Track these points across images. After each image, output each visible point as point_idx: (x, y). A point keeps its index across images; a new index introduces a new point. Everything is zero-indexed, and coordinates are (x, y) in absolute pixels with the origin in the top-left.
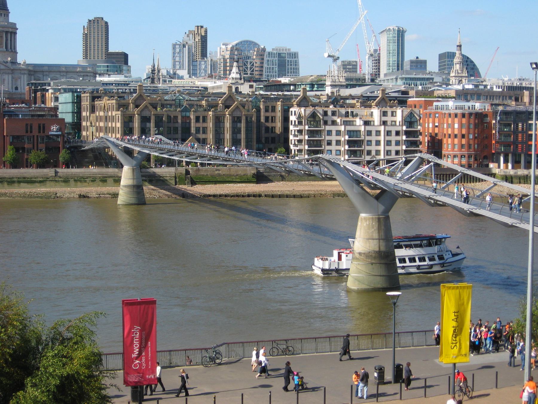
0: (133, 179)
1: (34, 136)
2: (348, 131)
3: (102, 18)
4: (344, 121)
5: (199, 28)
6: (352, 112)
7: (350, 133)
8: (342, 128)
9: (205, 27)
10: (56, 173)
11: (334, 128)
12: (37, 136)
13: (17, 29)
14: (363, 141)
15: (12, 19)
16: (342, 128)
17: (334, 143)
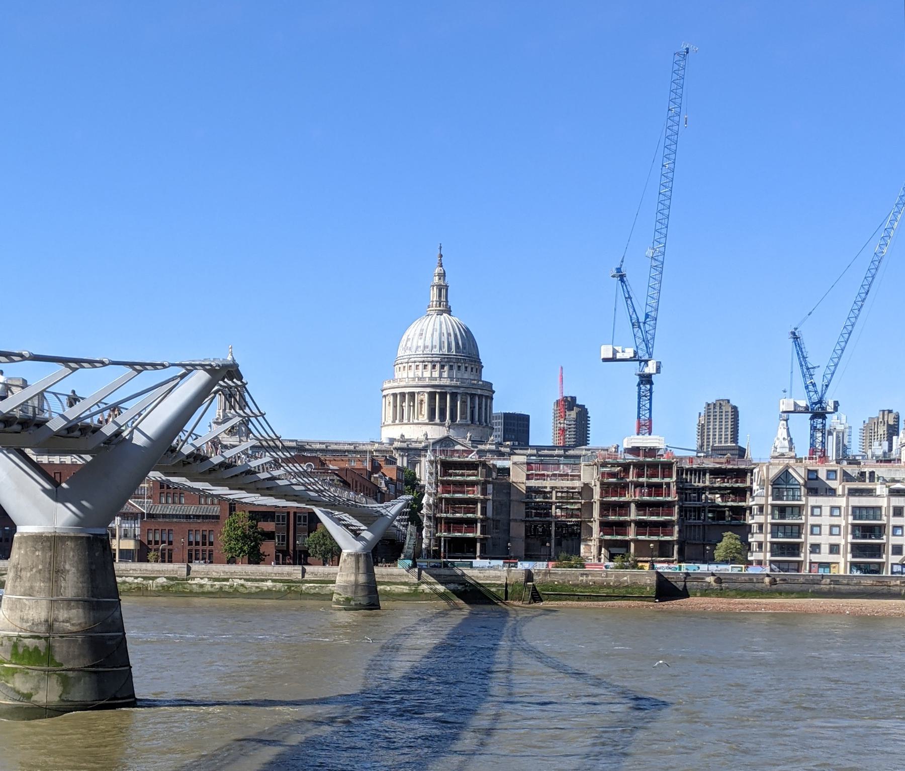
0: (356, 575)
1: (288, 513)
2: (854, 508)
3: (729, 401)
4: (849, 490)
5: (886, 413)
6: (872, 474)
7: (857, 511)
8: (841, 502)
9: (894, 412)
10: (304, 572)
11: (825, 502)
12: (295, 513)
13: (494, 392)
14: (884, 525)
15: (487, 376)
16: (841, 502)
17: (825, 530)
